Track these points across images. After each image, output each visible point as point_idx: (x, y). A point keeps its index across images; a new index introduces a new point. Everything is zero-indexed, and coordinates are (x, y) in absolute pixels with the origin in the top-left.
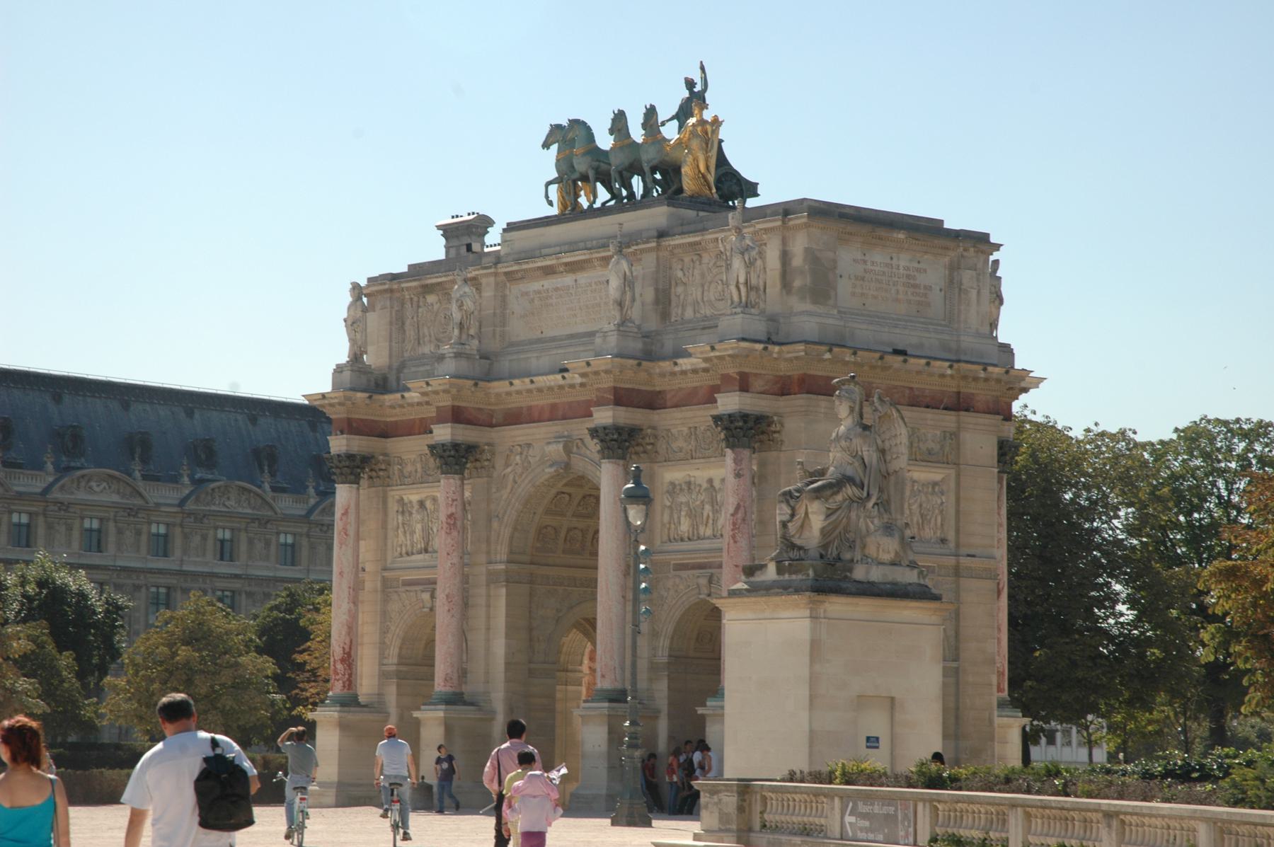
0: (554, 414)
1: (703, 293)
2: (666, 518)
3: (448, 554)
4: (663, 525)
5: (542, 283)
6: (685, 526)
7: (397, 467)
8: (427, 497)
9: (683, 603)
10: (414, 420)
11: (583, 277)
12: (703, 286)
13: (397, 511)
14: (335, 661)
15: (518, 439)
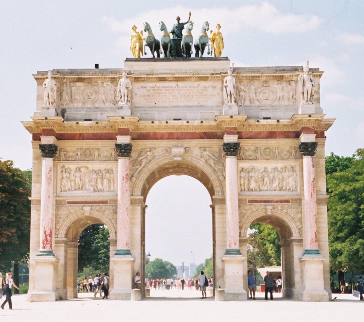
0: (170, 136)
1: (256, 96)
2: (242, 182)
3: (127, 191)
4: (241, 185)
5: (155, 84)
6: (253, 185)
7: (62, 153)
8: (81, 167)
9: (255, 216)
10: (75, 134)
11: (181, 84)
12: (256, 93)
13: (62, 171)
14: (46, 236)
15: (147, 146)
